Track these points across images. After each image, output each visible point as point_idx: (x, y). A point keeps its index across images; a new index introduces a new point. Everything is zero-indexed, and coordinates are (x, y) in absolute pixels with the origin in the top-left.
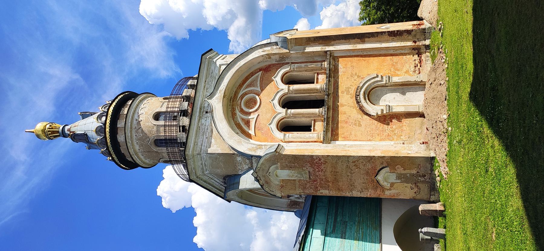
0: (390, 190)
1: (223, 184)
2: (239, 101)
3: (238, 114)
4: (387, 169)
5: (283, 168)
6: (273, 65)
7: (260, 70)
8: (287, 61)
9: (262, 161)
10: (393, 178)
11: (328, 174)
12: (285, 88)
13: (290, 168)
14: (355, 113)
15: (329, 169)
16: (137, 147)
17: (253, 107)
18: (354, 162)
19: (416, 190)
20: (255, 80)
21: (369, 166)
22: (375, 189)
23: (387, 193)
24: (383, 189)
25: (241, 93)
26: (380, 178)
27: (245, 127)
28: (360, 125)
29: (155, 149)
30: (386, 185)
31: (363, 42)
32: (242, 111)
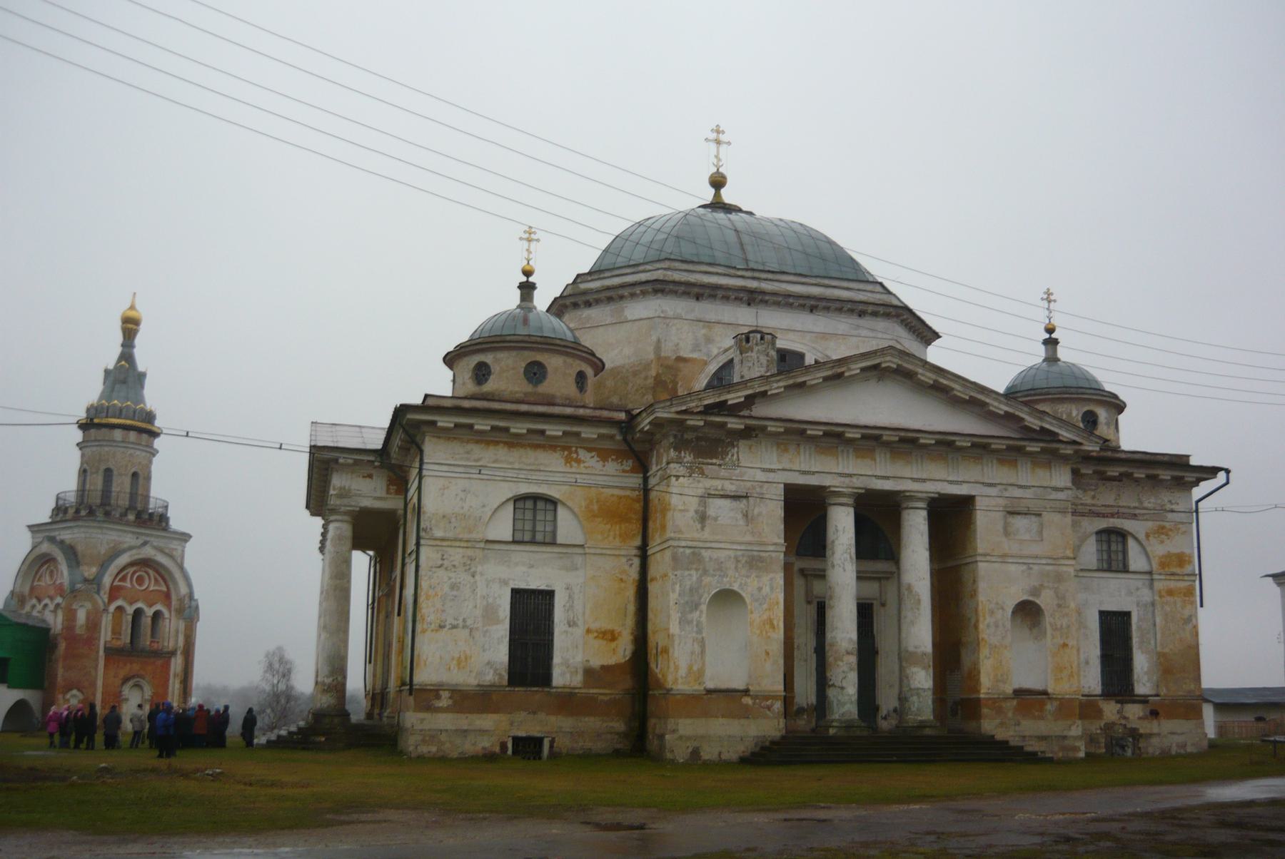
0: (64, 698)
1: (62, 537)
2: (143, 569)
3: (134, 568)
4: (81, 696)
6: (171, 603)
7: (168, 588)
8: (173, 613)
9: (96, 596)
10: (74, 702)
12: (150, 612)
13: (88, 618)
14: (123, 673)
16: (106, 449)
17: (136, 582)
18: (90, 672)
20: (159, 585)
23: (60, 696)
24: (65, 693)
25: (151, 572)
26: (75, 692)
27: (120, 576)
28: (115, 677)
29: (103, 467)
30: (68, 696)
31: (181, 683)
32: (134, 573)
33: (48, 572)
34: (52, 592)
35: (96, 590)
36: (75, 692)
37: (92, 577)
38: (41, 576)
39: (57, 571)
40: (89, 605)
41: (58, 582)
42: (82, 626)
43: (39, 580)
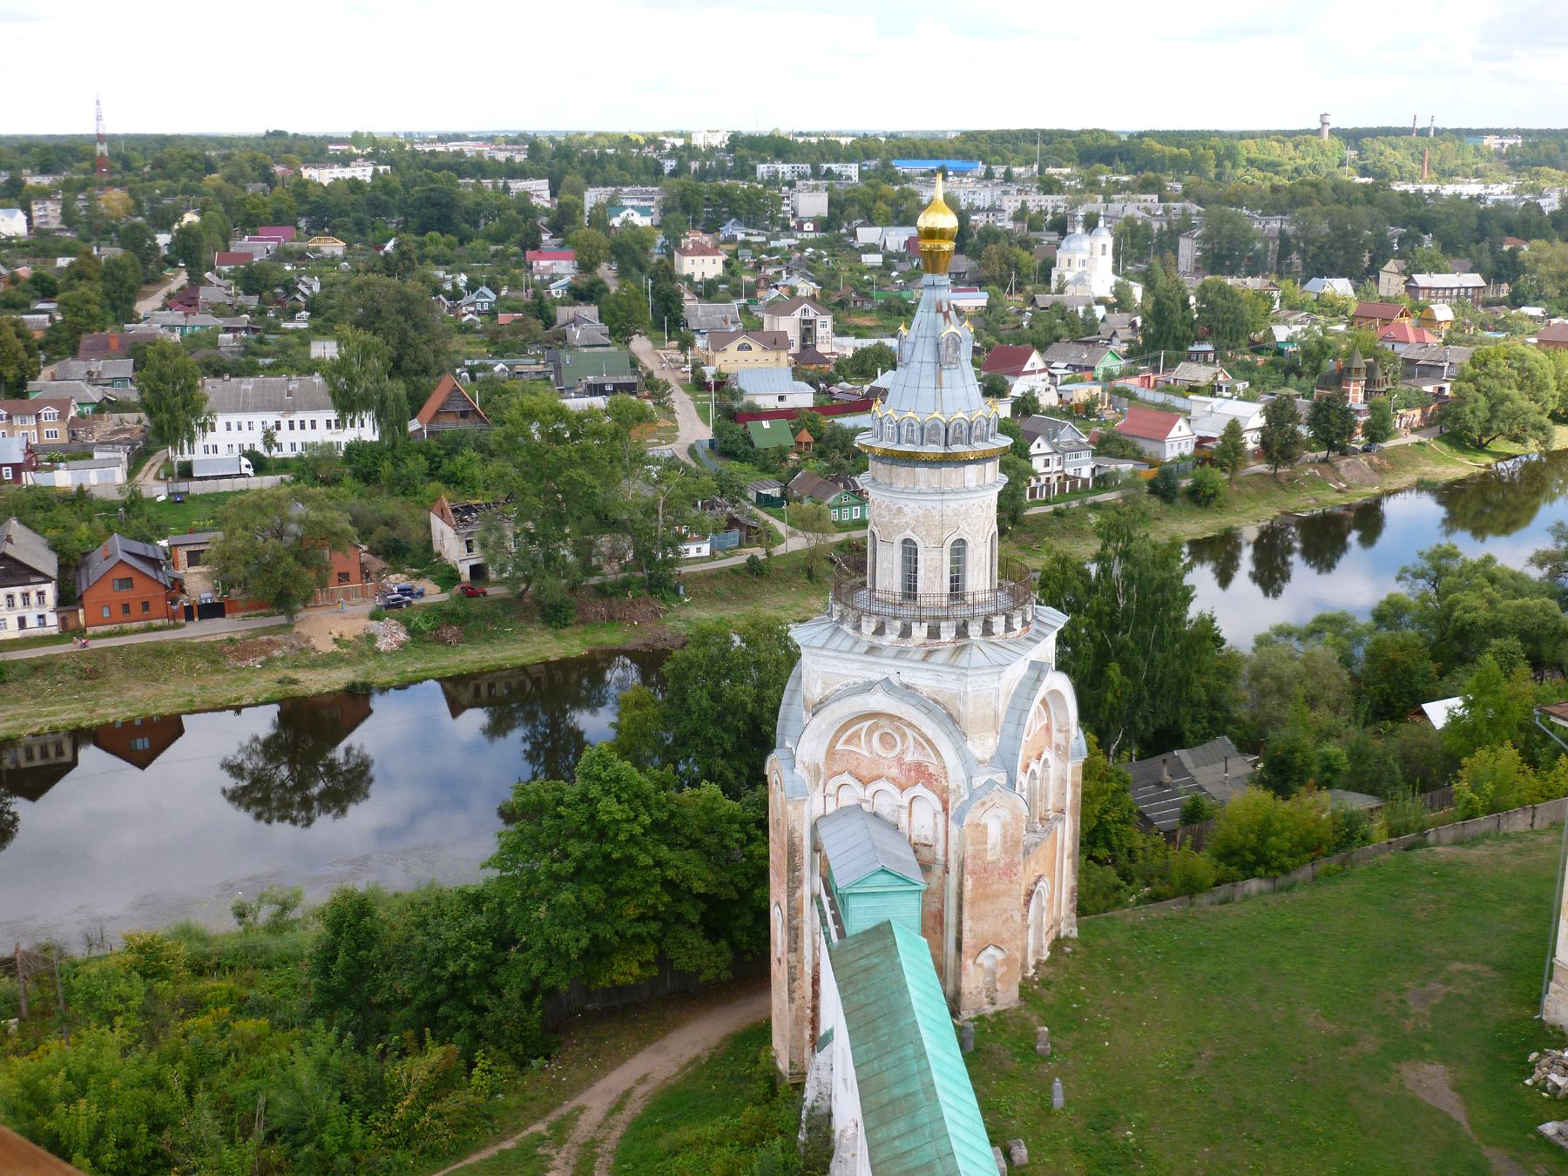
5: (1004, 826)
11: (995, 887)
15: (1002, 887)
19: (975, 992)
21: (1006, 935)
22: (974, 947)
26: (991, 950)
30: (979, 960)
33: (876, 736)
34: (894, 772)
35: (1004, 782)
36: (991, 950)
37: (988, 757)
38: (857, 735)
39: (903, 736)
40: (1005, 814)
41: (909, 758)
42: (994, 847)
43: (848, 741)
